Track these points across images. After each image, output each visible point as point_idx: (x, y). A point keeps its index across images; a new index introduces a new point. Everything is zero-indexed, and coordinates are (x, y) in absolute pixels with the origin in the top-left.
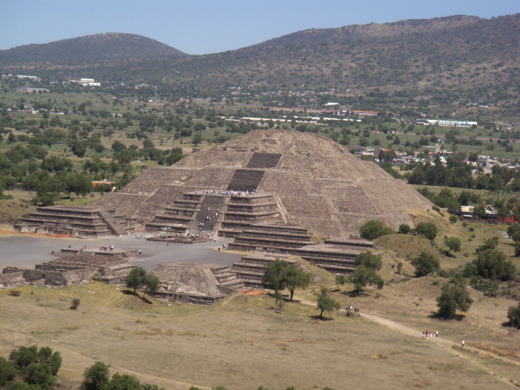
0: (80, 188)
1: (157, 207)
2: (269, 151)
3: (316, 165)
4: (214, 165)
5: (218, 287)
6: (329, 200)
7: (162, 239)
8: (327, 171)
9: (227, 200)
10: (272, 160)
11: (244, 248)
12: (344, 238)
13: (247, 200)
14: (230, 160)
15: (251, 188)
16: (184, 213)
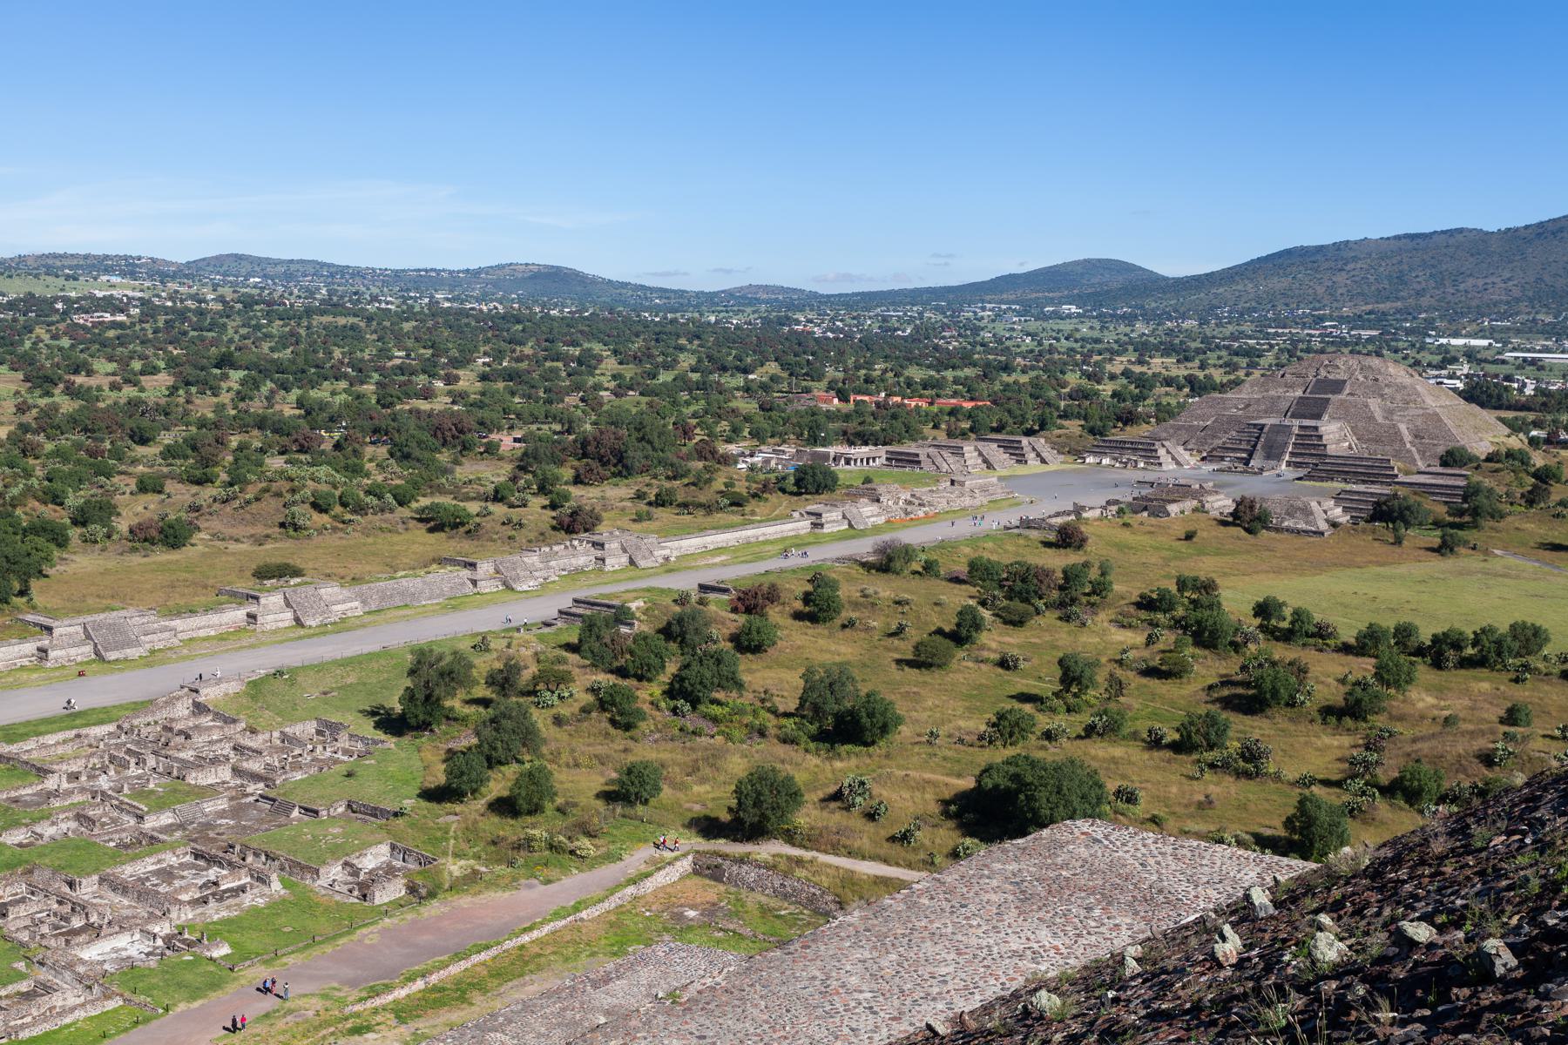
0: (1128, 419)
1: (1214, 437)
2: (1331, 377)
3: (1386, 390)
4: (1272, 393)
5: (1327, 521)
6: (1403, 427)
7: (1229, 470)
8: (1399, 397)
9: (1296, 430)
10: (1337, 386)
11: (1322, 479)
12: (1421, 465)
13: (1316, 428)
14: (1292, 386)
15: (1318, 417)
16: (1253, 444)
